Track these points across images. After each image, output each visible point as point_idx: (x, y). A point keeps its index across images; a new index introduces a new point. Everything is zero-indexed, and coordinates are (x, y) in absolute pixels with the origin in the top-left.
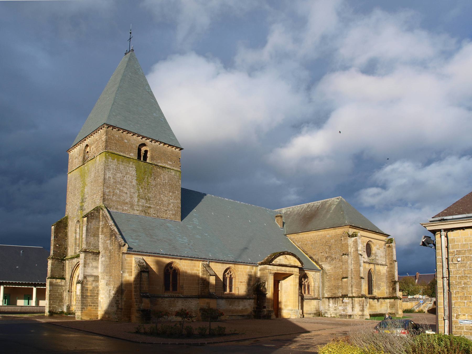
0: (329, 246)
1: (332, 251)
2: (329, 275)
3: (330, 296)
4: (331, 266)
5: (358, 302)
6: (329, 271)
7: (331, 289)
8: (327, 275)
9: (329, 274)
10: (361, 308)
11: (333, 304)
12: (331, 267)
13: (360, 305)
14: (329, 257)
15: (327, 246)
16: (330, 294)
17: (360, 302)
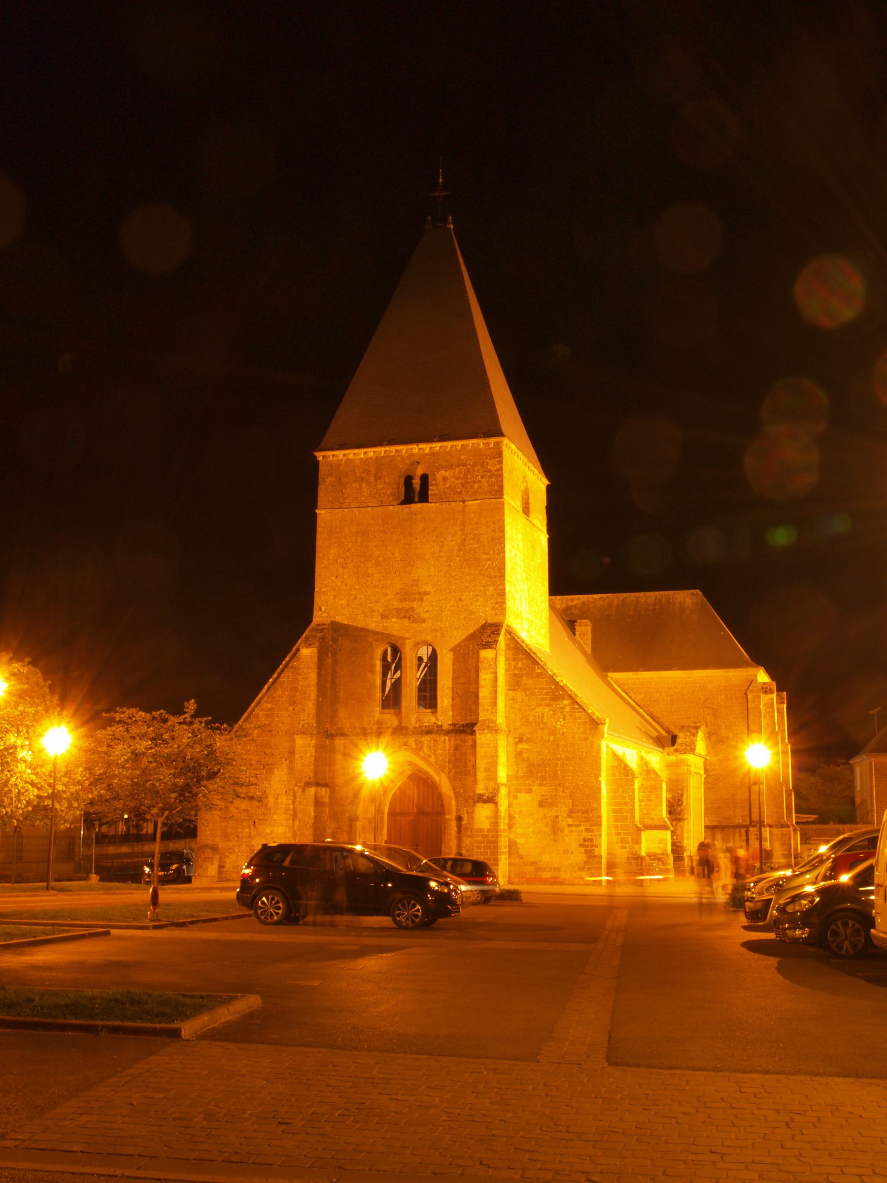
0: (713, 709)
1: (719, 720)
2: (714, 775)
3: (715, 824)
4: (717, 756)
5: (780, 836)
6: (713, 767)
7: (719, 808)
8: (710, 775)
9: (713, 773)
10: (786, 851)
11: (723, 840)
12: (718, 758)
13: (783, 844)
14: (713, 734)
15: (708, 708)
16: (717, 819)
17: (784, 838)
